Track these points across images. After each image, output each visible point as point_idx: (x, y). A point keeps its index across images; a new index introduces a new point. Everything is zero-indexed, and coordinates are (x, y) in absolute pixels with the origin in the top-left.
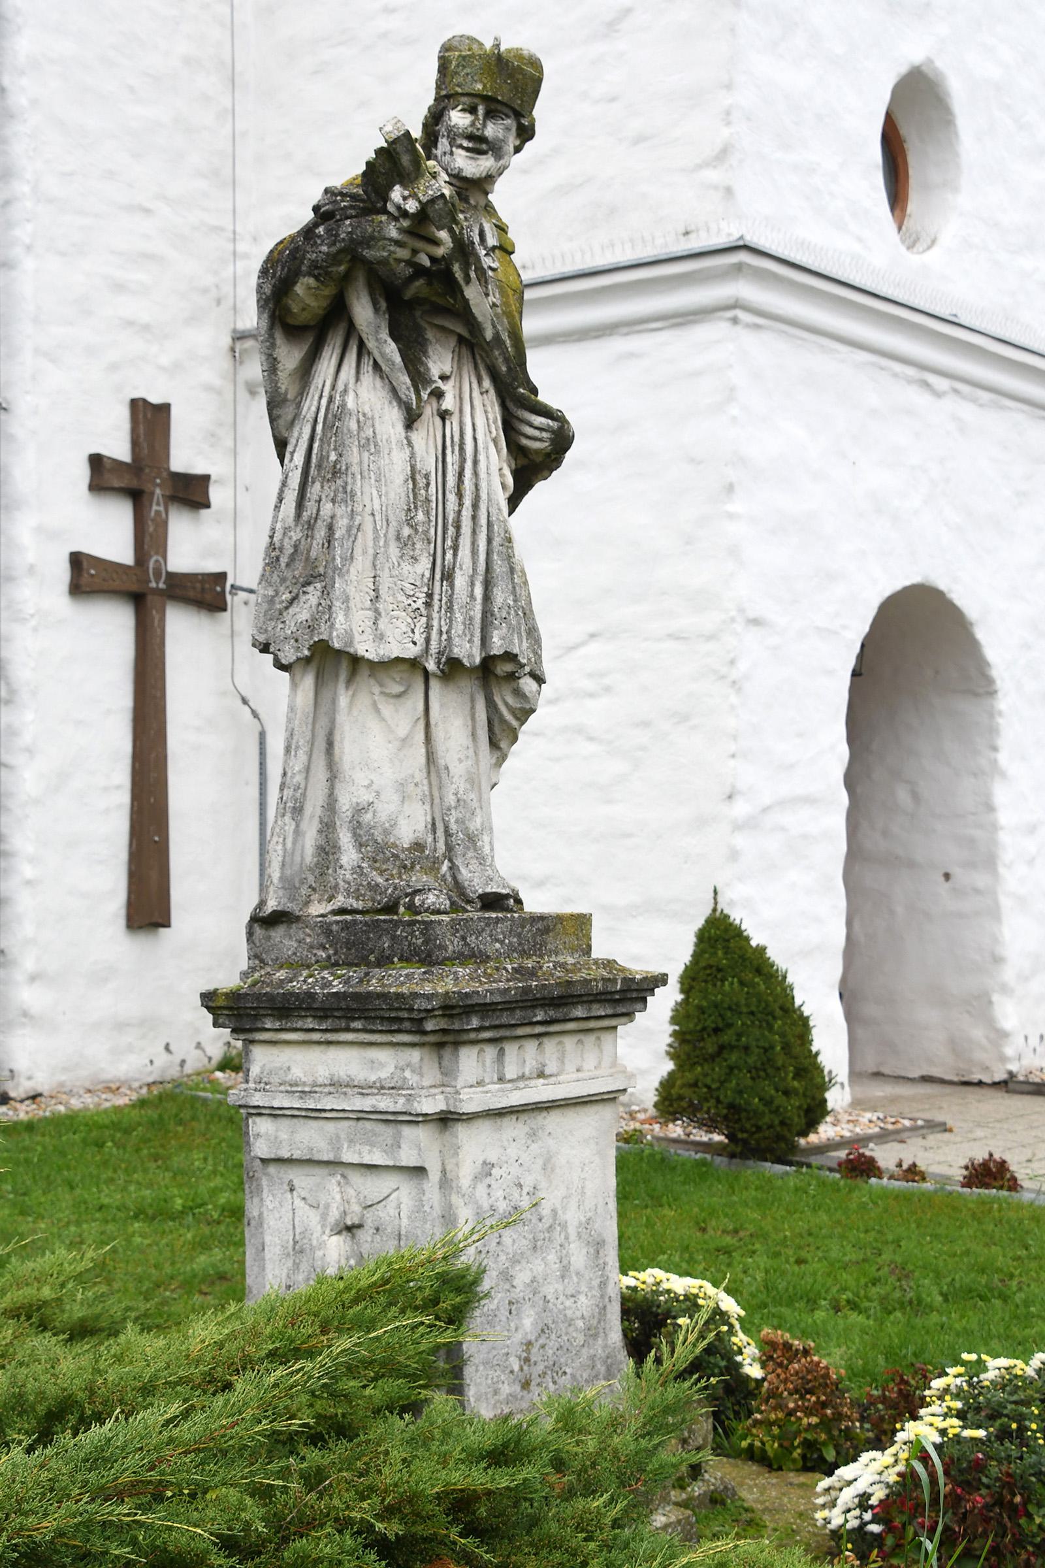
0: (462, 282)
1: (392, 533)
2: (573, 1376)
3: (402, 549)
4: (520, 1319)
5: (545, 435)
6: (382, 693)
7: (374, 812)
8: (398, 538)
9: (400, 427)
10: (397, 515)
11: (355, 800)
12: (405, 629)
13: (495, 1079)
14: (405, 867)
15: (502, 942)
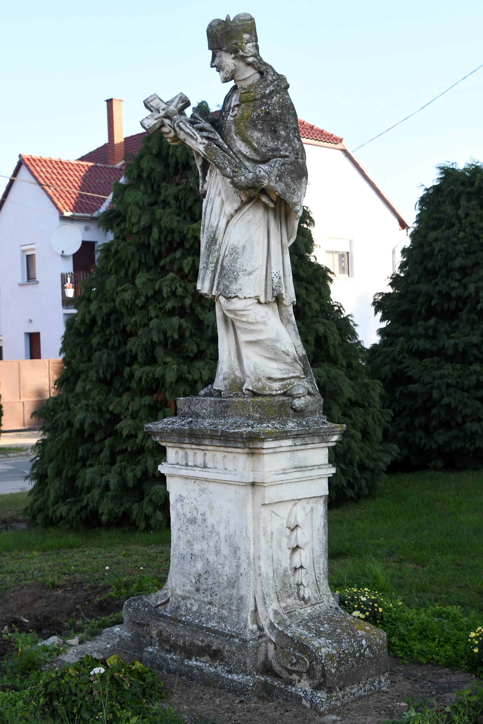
2: (220, 599)
4: (196, 563)
13: (184, 463)
15: (206, 410)
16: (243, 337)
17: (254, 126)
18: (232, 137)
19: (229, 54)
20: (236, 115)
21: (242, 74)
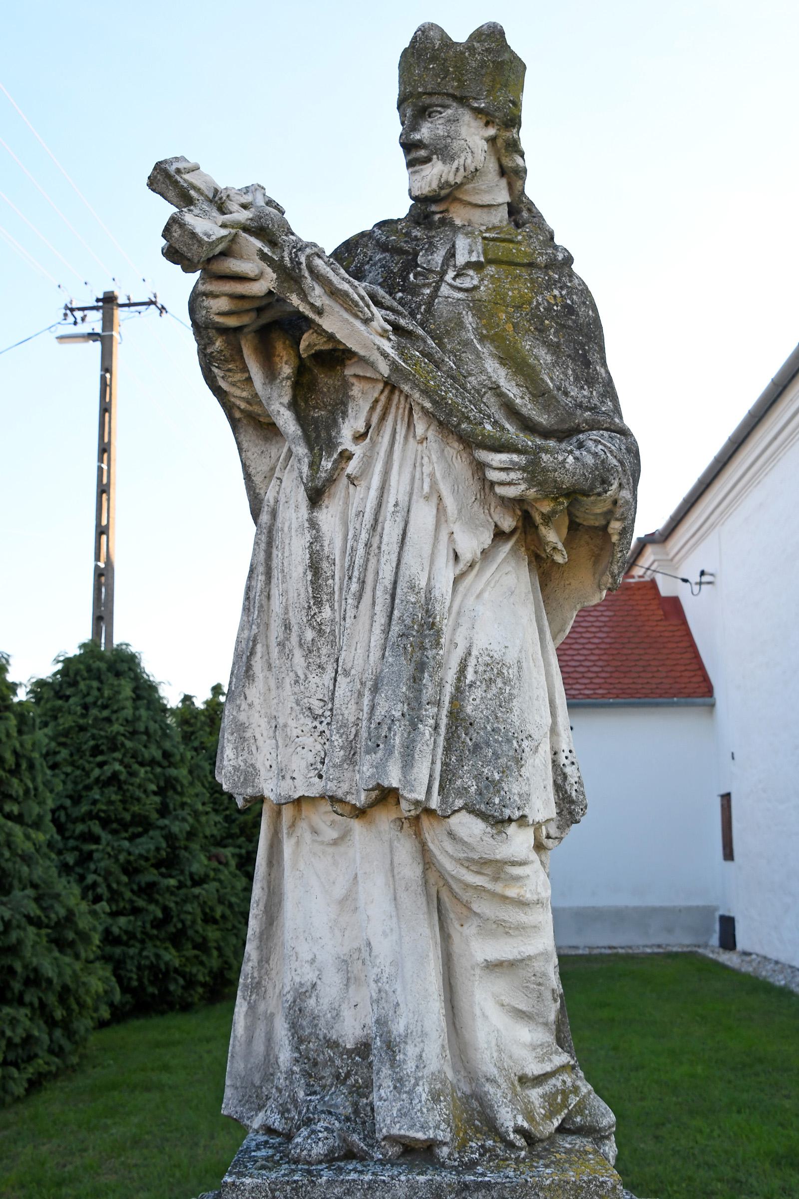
0: (311, 315)
1: (294, 639)
3: (306, 657)
5: (513, 476)
6: (314, 841)
7: (317, 997)
8: (301, 645)
9: (304, 512)
10: (297, 618)
11: (297, 979)
12: (313, 761)
14: (338, 1076)
16: (478, 948)
17: (540, 331)
18: (467, 343)
19: (481, 123)
20: (475, 288)
21: (489, 191)
